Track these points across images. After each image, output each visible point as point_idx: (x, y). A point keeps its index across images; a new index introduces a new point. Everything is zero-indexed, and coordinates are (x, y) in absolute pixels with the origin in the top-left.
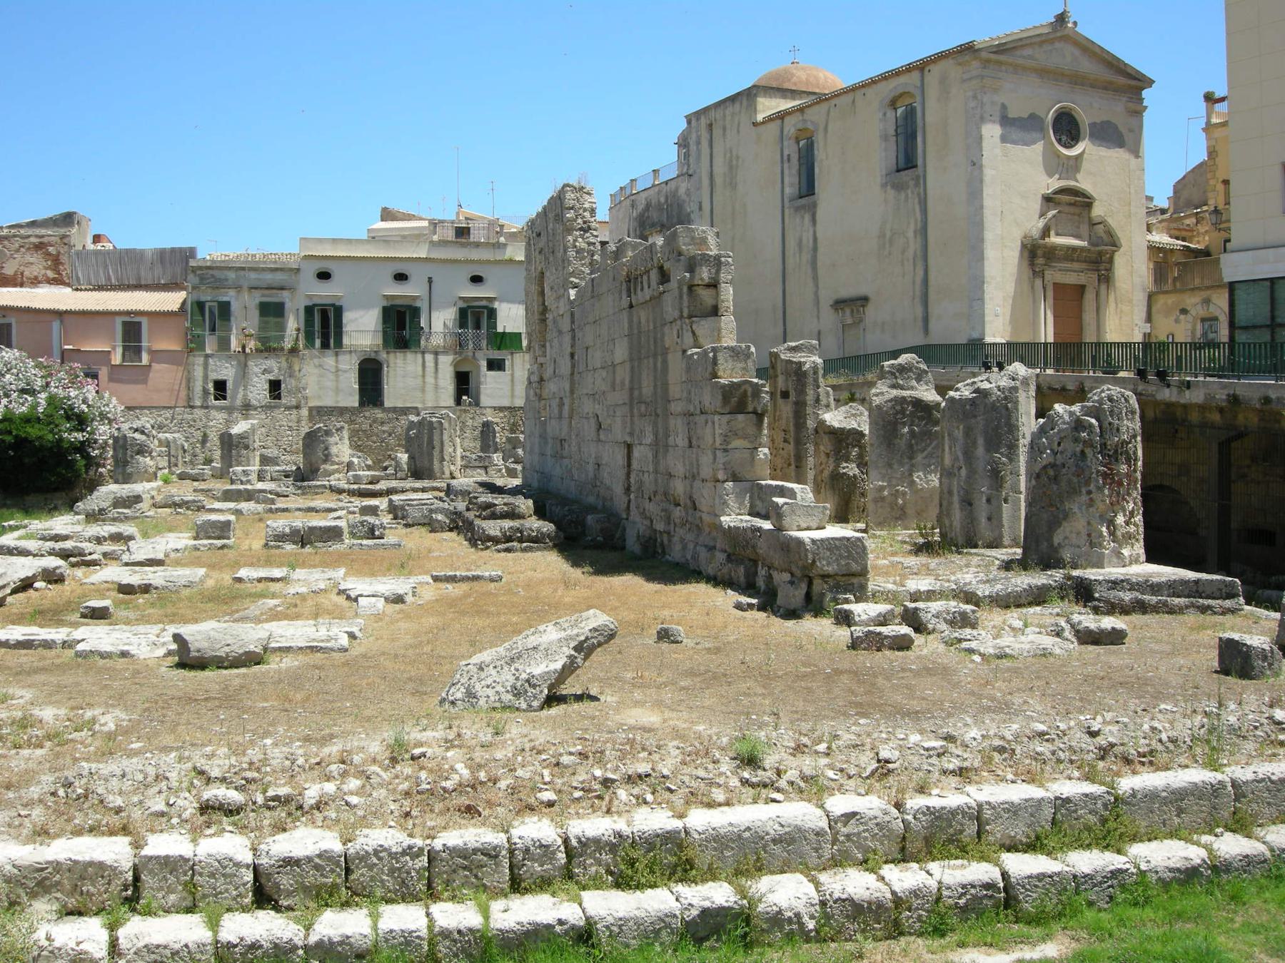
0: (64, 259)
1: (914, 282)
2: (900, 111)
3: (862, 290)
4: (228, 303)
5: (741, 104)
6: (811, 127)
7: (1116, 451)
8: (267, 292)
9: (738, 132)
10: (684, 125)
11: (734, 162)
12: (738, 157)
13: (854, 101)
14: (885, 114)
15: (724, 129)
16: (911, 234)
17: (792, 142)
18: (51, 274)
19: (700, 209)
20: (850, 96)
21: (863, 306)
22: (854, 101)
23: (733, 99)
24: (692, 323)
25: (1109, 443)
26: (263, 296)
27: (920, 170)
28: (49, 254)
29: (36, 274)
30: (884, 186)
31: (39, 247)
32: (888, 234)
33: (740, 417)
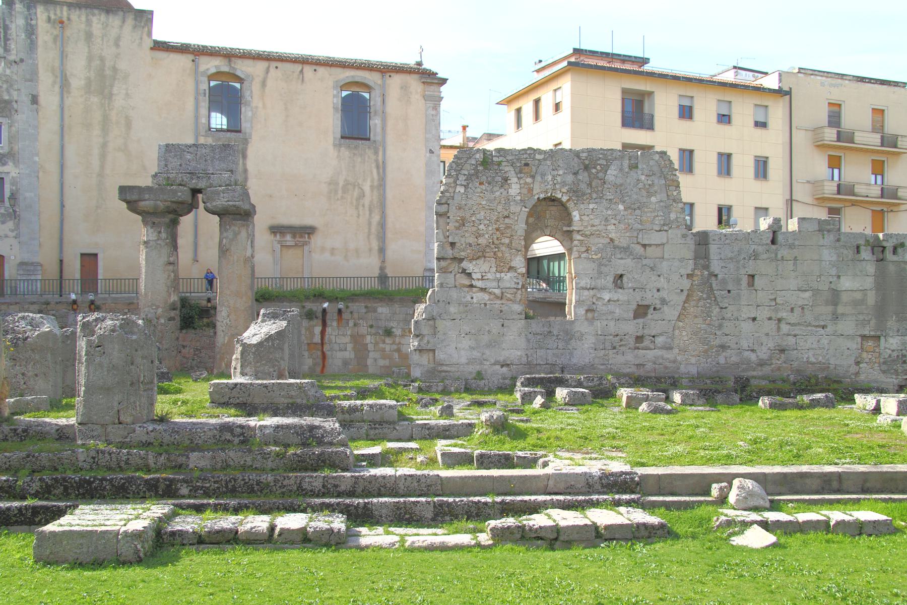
1: (370, 224)
2: (344, 94)
3: (308, 221)
5: (124, 21)
6: (242, 76)
9: (117, 45)
11: (108, 72)
12: (115, 69)
13: (302, 71)
15: (89, 36)
16: (367, 188)
17: (206, 79)
19: (35, 100)
20: (298, 67)
22: (302, 71)
30: (337, 146)
32: (341, 183)
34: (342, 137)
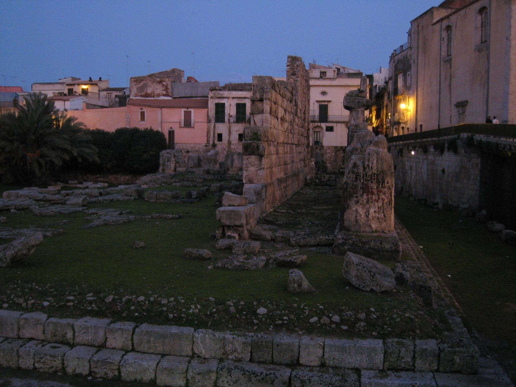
0: (169, 87)
4: (224, 104)
6: (451, 25)
7: (371, 178)
8: (239, 99)
10: (410, 26)
14: (476, 17)
18: (164, 93)
19: (414, 62)
21: (466, 105)
23: (426, 13)
24: (254, 117)
25: (368, 174)
26: (238, 101)
27: (488, 42)
28: (164, 85)
29: (159, 92)
31: (160, 82)
33: (253, 157)
34: (482, 43)
